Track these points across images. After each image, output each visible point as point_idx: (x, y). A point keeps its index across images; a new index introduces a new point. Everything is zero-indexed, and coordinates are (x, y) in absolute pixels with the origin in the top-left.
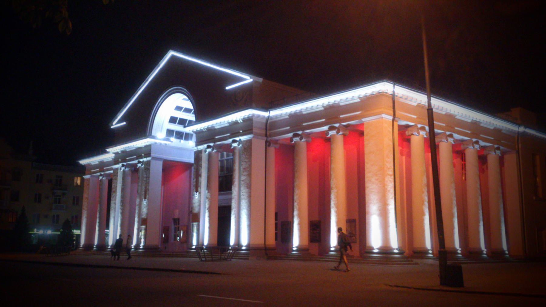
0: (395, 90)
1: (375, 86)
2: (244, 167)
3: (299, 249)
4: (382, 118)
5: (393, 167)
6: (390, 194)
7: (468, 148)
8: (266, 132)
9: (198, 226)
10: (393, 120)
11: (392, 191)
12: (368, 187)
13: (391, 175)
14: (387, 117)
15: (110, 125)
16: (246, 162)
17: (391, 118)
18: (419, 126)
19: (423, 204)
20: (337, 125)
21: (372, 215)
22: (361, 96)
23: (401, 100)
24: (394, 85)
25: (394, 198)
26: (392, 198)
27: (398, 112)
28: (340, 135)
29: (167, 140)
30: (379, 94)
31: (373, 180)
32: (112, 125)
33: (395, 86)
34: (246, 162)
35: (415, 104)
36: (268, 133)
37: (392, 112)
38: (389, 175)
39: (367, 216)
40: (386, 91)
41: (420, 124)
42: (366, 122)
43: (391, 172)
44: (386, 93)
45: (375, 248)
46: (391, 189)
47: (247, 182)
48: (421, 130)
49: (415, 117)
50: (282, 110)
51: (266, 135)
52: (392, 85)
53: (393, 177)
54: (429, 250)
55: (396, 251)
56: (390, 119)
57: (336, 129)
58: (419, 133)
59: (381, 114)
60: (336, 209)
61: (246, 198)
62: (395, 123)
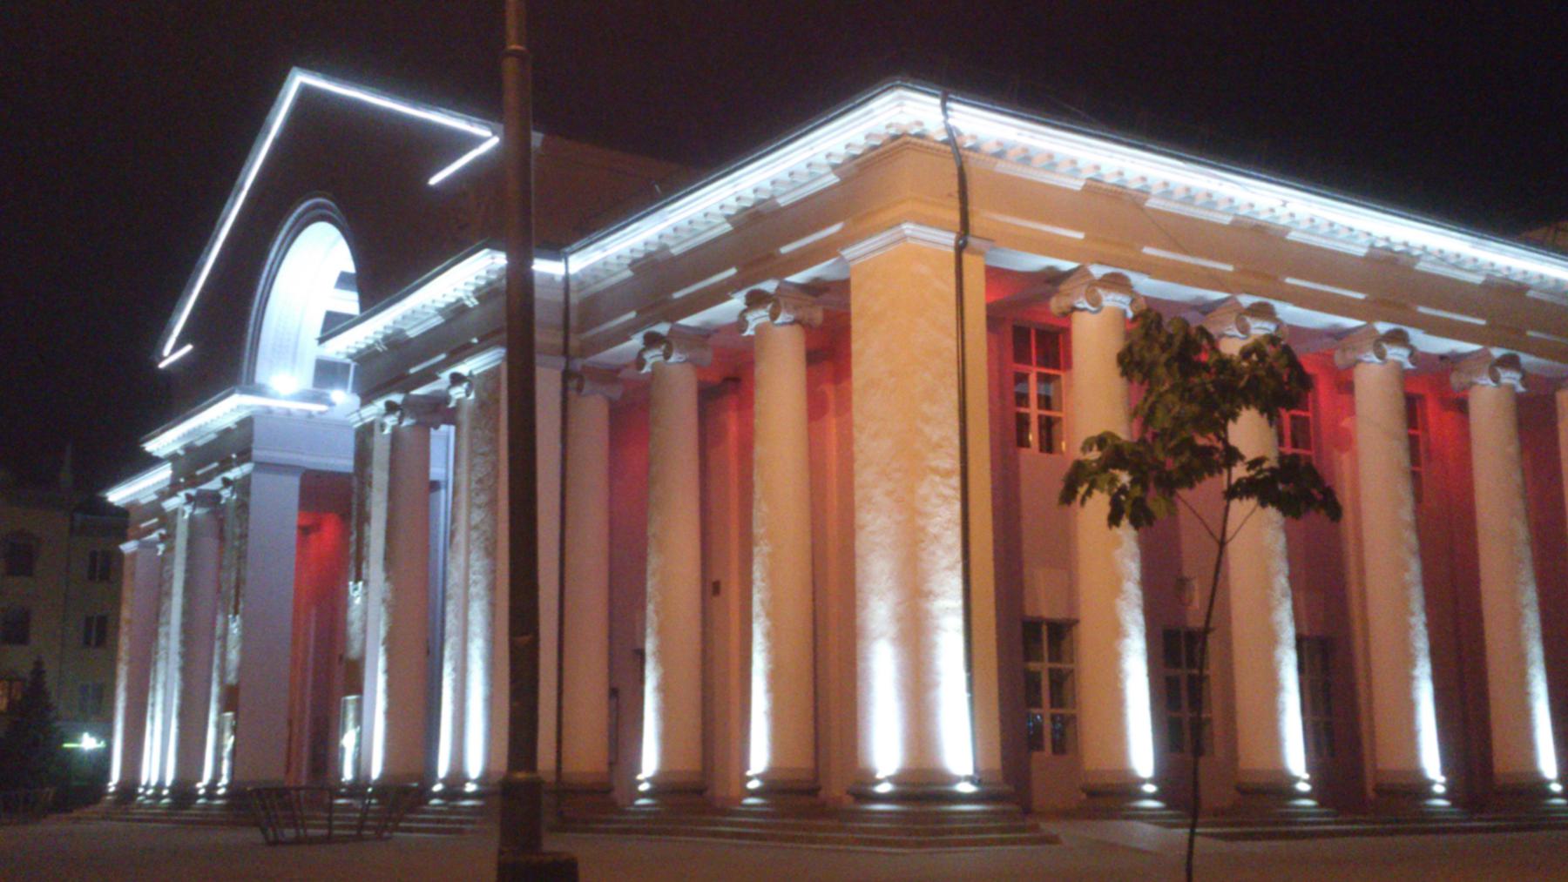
0: (942, 118)
1: (871, 111)
2: (480, 475)
3: (661, 787)
4: (904, 238)
5: (956, 442)
6: (940, 553)
7: (1360, 361)
8: (566, 339)
9: (359, 703)
10: (960, 249)
11: (953, 537)
12: (862, 527)
13: (947, 474)
14: (929, 237)
15: (157, 359)
16: (483, 454)
17: (948, 239)
18: (1098, 271)
19: (1117, 590)
20: (769, 286)
21: (875, 639)
22: (838, 161)
23: (1002, 167)
24: (945, 100)
25: (959, 566)
26: (950, 568)
27: (981, 218)
28: (784, 324)
29: (317, 399)
30: (896, 143)
31: (878, 495)
32: (162, 359)
33: (949, 104)
34: (483, 454)
35: (1077, 185)
36: (574, 342)
37: (955, 216)
38: (936, 471)
39: (860, 644)
40: (916, 130)
41: (1101, 263)
42: (857, 262)
43: (951, 462)
44: (920, 136)
45: (879, 776)
46: (947, 529)
47: (485, 532)
48: (1104, 287)
49: (1080, 235)
50: (603, 249)
51: (565, 351)
52: (937, 101)
53: (956, 481)
54: (1143, 781)
55: (966, 788)
56: (946, 245)
57: (769, 302)
58: (1096, 302)
59: (899, 224)
60: (768, 623)
61: (482, 593)
62: (968, 258)
